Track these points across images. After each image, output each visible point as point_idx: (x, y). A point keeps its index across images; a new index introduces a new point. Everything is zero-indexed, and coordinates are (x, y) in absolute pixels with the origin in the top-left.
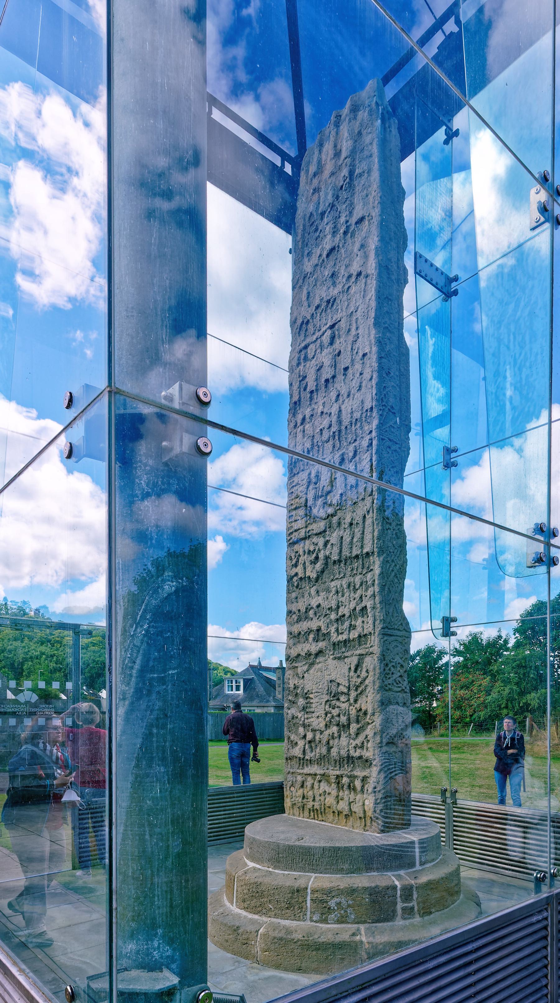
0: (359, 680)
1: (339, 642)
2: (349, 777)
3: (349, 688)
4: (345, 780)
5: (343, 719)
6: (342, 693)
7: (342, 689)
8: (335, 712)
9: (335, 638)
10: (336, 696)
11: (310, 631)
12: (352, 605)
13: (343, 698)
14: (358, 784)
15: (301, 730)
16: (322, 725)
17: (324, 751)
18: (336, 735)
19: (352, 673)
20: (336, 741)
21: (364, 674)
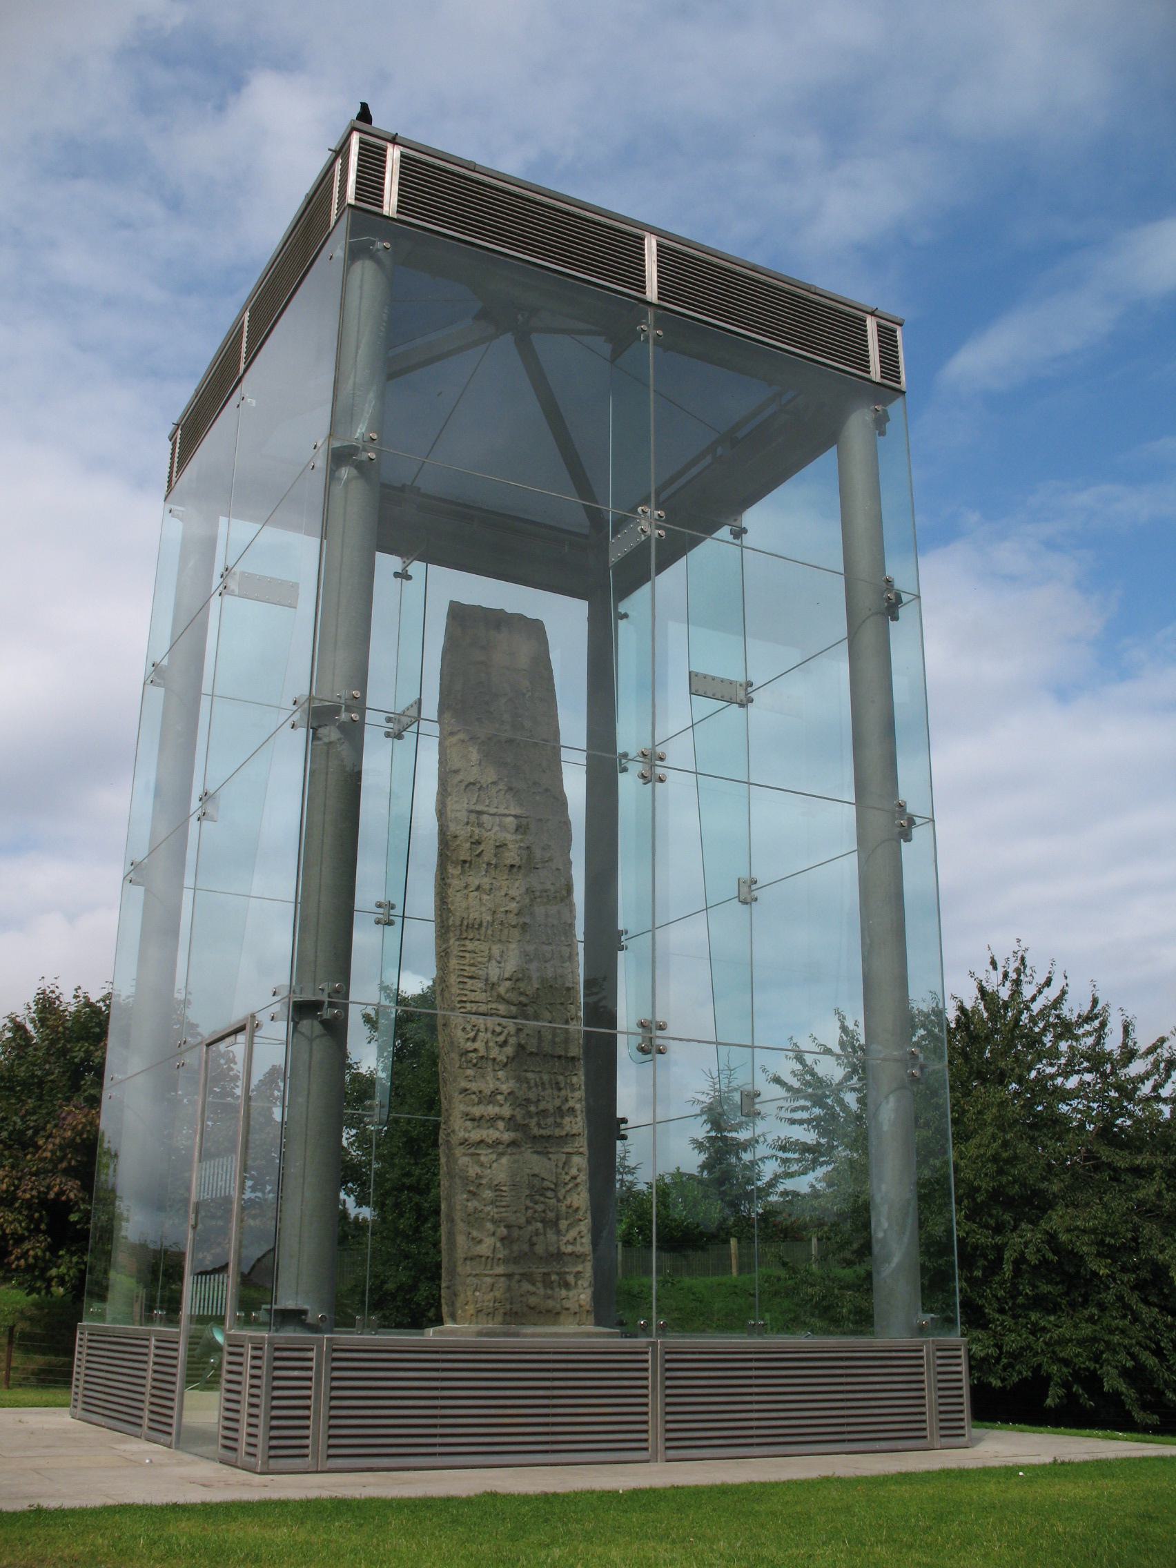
0: (568, 1178)
1: (542, 1136)
2: (558, 1274)
3: (556, 1185)
4: (554, 1277)
5: (551, 1215)
6: (549, 1189)
7: (546, 1184)
8: (539, 1208)
9: (536, 1131)
10: (542, 1191)
11: (499, 1117)
12: (557, 1103)
13: (549, 1194)
14: (571, 1279)
15: (489, 1226)
16: (522, 1220)
17: (526, 1247)
18: (541, 1231)
19: (560, 1170)
20: (542, 1237)
21: (574, 1171)
